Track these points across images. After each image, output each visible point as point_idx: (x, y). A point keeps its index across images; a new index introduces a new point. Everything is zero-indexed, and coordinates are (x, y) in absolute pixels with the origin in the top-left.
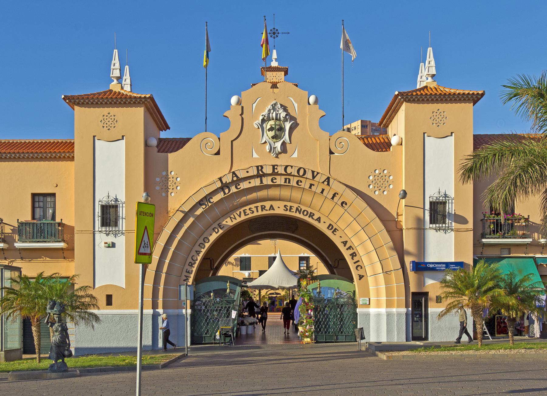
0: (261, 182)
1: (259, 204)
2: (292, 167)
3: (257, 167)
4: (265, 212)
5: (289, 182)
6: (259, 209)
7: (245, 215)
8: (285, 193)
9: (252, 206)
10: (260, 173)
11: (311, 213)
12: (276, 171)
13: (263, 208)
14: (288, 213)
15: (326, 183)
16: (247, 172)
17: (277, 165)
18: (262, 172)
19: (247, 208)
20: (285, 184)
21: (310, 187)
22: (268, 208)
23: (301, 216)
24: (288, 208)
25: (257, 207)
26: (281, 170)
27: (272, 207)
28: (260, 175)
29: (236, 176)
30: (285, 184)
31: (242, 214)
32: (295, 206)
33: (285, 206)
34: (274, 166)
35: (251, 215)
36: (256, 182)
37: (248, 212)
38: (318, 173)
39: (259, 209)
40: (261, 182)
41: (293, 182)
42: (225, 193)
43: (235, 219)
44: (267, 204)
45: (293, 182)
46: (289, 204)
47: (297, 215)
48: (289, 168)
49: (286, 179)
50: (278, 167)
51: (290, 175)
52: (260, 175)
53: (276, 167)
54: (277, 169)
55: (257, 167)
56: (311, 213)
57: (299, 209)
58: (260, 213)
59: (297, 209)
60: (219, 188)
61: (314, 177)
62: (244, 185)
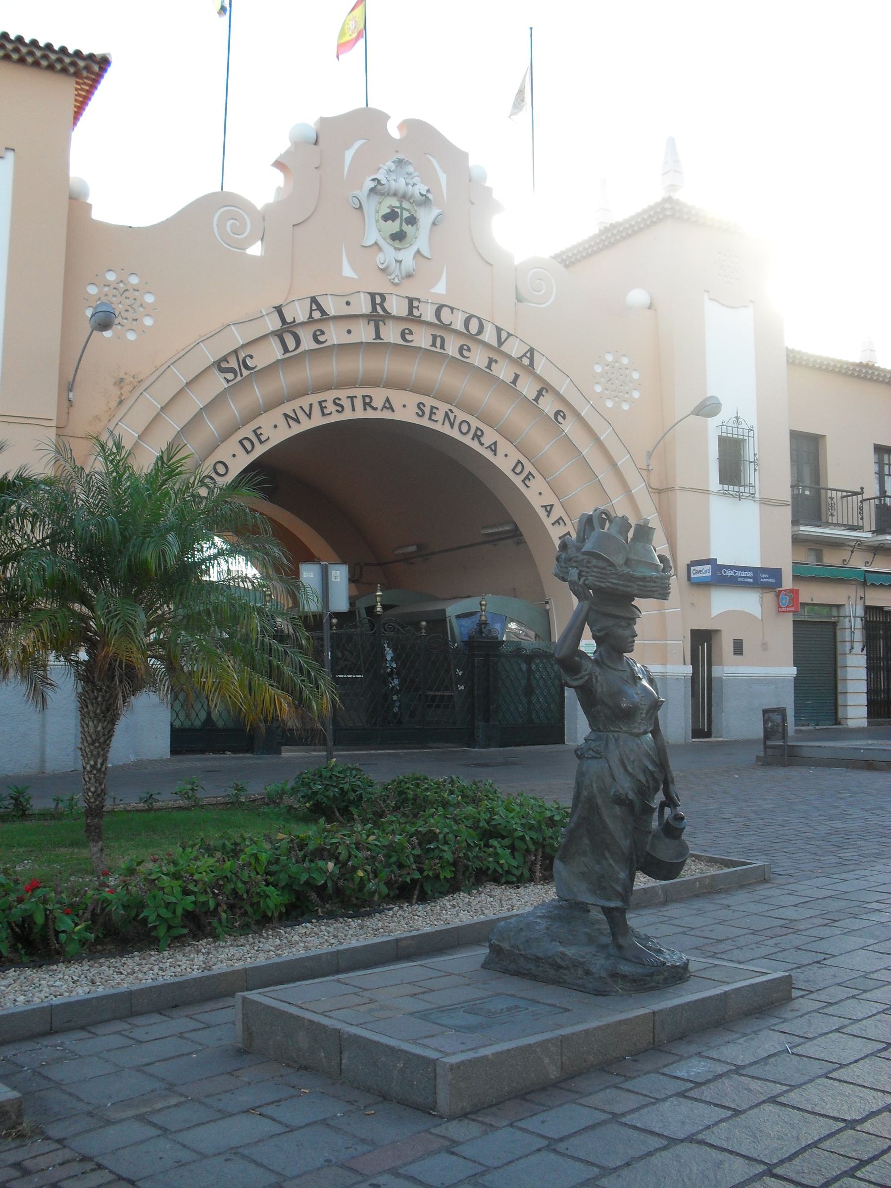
0: (378, 336)
1: (359, 392)
2: (452, 309)
3: (373, 296)
4: (370, 414)
5: (442, 347)
6: (359, 403)
7: (324, 414)
8: (415, 369)
9: (343, 394)
10: (379, 308)
11: (477, 428)
12: (416, 313)
13: (367, 403)
14: (425, 422)
15: (526, 361)
16: (348, 303)
17: (418, 300)
18: (384, 309)
19: (330, 396)
20: (433, 349)
21: (489, 367)
22: (378, 402)
23: (455, 434)
24: (427, 410)
25: (352, 398)
26: (428, 314)
27: (388, 405)
28: (378, 316)
29: (320, 308)
30: (433, 349)
31: (316, 410)
32: (443, 407)
33: (420, 405)
34: (411, 301)
35: (335, 418)
36: (364, 333)
37: (331, 408)
38: (509, 335)
39: (359, 403)
40: (378, 336)
41: (452, 348)
42: (286, 350)
43: (297, 421)
44: (379, 396)
45: (452, 348)
46: (429, 402)
47: (446, 430)
48: (445, 313)
49: (434, 337)
50: (421, 306)
51: (447, 327)
52: (378, 316)
53: (415, 304)
54: (417, 308)
55: (373, 296)
56: (477, 428)
57: (452, 416)
58: (360, 414)
59: (447, 415)
60: (274, 333)
61: (500, 343)
62: (334, 335)
